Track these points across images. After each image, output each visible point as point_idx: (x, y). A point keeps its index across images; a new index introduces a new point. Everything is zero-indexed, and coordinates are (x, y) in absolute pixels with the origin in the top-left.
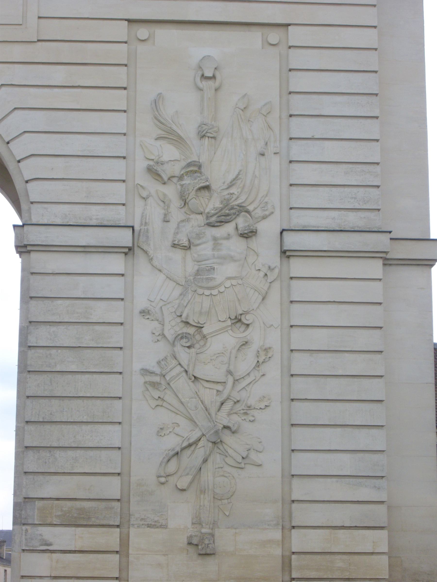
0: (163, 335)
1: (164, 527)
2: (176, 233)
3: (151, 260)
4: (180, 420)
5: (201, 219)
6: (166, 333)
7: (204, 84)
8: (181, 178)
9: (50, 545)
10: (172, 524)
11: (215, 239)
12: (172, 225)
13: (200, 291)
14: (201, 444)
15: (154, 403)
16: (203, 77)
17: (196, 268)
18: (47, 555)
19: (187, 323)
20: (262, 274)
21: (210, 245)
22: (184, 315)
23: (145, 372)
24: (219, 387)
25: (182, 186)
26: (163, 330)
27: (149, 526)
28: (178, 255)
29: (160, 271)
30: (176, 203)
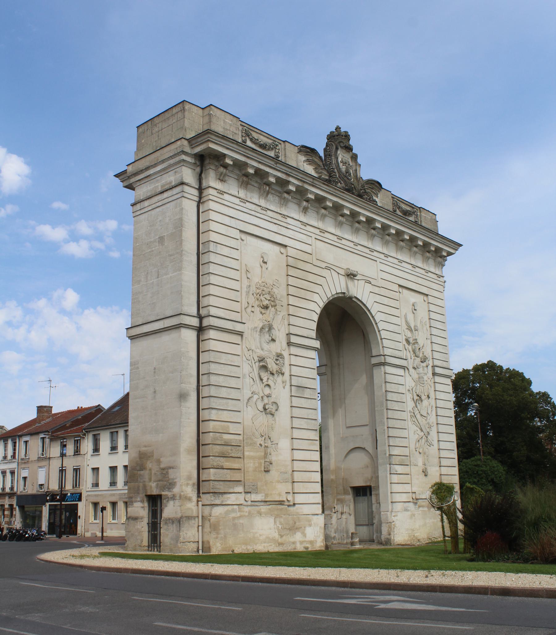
0: (413, 399)
1: (417, 466)
2: (413, 363)
3: (409, 373)
4: (419, 430)
5: (418, 360)
6: (414, 398)
7: (414, 311)
8: (414, 344)
9: (397, 472)
11: (423, 367)
12: (412, 360)
13: (421, 385)
14: (423, 437)
15: (413, 422)
17: (418, 376)
18: (397, 475)
20: (430, 380)
21: (421, 369)
22: (417, 393)
23: (410, 412)
24: (425, 418)
25: (415, 347)
26: (413, 397)
27: (415, 465)
28: (413, 370)
29: (411, 376)
30: (412, 353)
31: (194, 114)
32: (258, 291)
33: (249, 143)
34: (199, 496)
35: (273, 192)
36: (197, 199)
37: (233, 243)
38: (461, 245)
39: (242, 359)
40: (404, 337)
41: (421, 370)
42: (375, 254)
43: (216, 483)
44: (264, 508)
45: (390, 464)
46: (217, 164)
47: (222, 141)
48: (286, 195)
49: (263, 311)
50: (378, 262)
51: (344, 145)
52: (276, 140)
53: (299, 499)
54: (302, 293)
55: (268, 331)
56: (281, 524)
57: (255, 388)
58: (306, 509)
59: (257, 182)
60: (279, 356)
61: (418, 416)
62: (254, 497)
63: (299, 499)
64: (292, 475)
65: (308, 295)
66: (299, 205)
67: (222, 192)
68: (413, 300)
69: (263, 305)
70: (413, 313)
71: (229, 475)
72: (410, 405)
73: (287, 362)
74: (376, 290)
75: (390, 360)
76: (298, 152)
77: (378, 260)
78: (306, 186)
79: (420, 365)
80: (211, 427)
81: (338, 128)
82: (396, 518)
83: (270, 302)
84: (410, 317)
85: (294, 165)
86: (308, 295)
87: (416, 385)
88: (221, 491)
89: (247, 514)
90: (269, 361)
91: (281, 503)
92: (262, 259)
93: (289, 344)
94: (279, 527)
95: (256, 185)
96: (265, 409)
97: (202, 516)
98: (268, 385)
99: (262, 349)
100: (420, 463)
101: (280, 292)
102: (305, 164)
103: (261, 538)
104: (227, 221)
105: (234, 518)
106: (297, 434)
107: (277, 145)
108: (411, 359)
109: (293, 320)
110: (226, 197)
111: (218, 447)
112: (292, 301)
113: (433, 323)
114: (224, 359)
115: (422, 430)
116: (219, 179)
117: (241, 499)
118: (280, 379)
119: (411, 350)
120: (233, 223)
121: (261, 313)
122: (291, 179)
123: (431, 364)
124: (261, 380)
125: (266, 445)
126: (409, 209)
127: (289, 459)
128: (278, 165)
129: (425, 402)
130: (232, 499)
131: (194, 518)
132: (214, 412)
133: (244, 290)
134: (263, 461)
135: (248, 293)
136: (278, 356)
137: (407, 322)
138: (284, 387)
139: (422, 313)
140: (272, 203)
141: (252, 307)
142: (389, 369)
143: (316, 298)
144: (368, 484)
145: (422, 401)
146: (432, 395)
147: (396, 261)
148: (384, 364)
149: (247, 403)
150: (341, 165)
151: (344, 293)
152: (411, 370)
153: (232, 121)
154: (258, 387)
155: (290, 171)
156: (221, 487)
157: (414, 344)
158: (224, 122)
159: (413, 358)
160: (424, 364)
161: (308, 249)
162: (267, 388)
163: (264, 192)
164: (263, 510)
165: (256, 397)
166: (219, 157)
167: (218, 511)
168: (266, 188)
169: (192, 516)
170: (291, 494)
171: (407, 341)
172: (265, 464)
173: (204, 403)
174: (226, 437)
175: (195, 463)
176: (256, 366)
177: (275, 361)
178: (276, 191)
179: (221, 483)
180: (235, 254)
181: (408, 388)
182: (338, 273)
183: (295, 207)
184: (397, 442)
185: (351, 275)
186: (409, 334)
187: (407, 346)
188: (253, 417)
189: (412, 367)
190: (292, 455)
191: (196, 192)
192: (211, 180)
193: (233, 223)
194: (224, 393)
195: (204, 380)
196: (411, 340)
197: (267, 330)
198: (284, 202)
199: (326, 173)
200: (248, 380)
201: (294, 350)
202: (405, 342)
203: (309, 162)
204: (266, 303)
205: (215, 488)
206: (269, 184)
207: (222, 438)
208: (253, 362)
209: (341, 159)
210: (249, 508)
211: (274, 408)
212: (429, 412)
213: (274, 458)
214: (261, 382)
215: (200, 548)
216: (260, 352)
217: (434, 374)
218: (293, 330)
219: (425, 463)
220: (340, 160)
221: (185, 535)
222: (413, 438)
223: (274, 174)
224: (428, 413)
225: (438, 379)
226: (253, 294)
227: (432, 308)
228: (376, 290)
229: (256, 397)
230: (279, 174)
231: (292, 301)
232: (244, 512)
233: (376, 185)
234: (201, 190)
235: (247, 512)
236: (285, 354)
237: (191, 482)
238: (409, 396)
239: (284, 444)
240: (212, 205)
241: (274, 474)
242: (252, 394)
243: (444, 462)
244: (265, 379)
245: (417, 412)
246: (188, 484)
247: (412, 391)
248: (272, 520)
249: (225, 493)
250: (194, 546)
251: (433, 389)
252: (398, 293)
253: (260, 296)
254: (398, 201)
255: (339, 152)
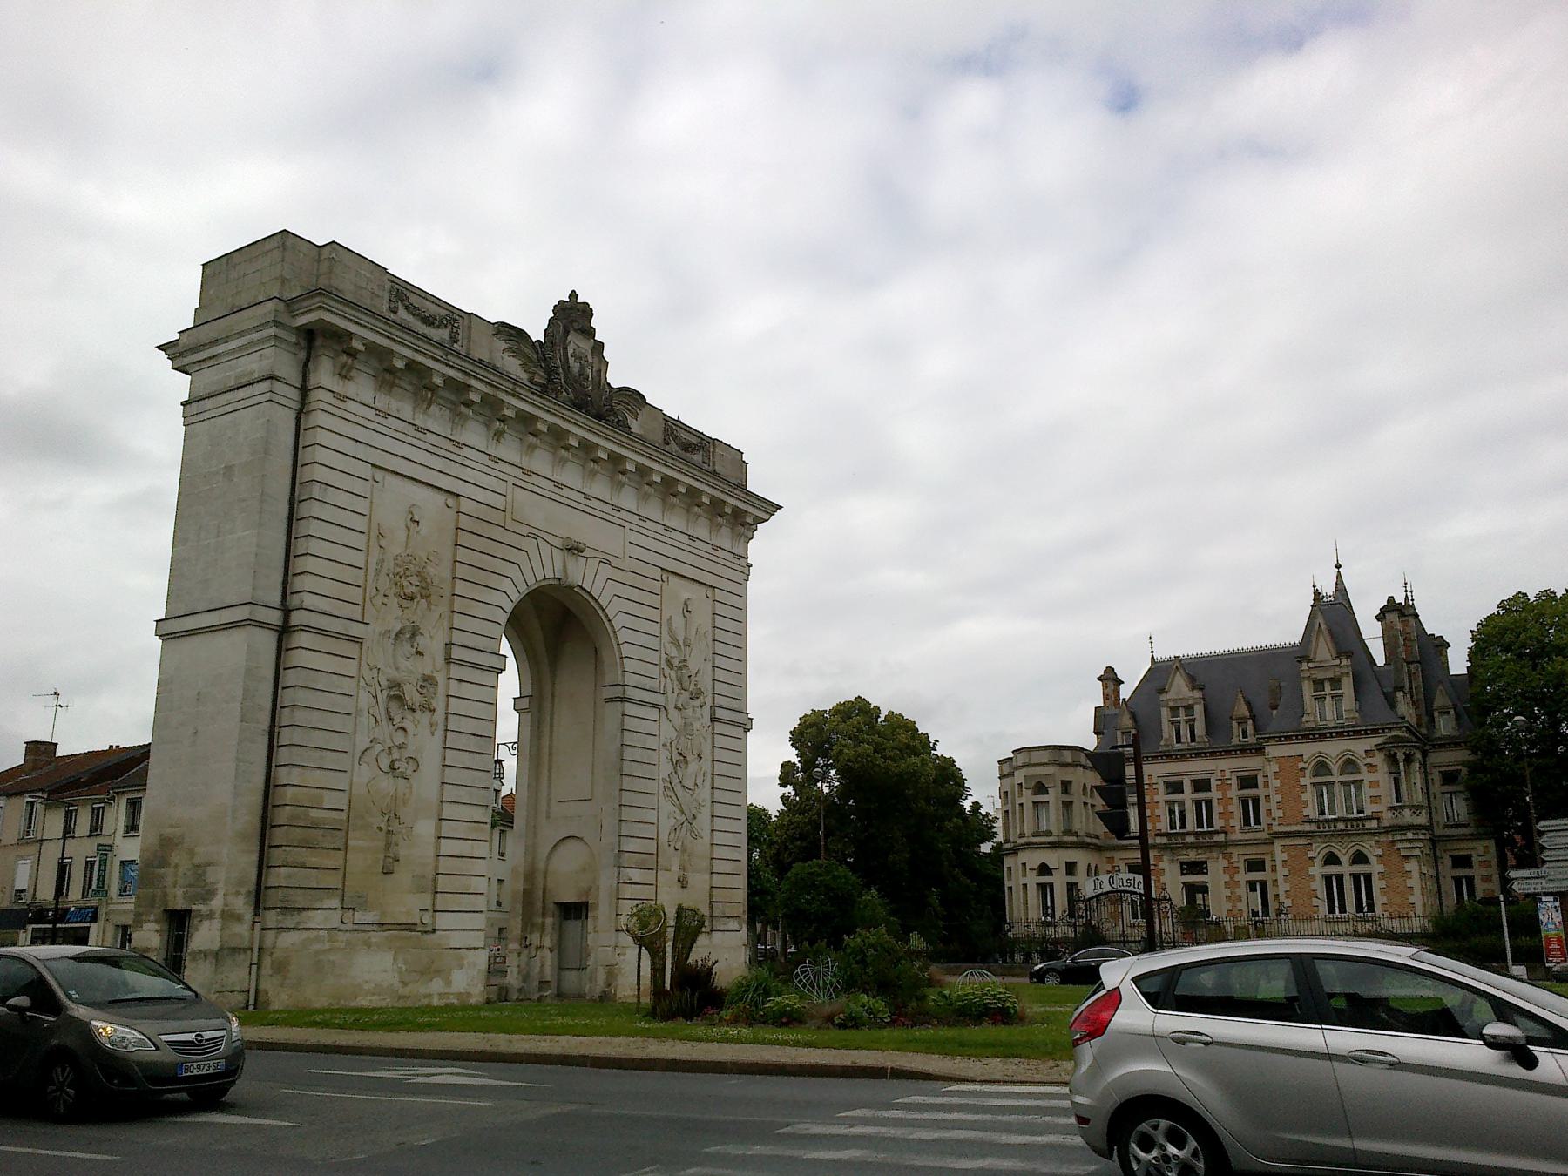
0: (671, 759)
1: (670, 870)
2: (677, 701)
4: (678, 811)
5: (687, 694)
7: (686, 614)
8: (680, 668)
10: (672, 870)
11: (693, 707)
16: (687, 611)
19: (681, 754)
21: (691, 710)
23: (664, 780)
30: (676, 683)
31: (302, 255)
32: (398, 570)
33: (403, 314)
34: (256, 914)
35: (442, 402)
36: (296, 406)
37: (358, 486)
38: (781, 507)
39: (358, 685)
40: (664, 656)
41: (689, 712)
42: (623, 514)
43: (291, 891)
44: (377, 937)
45: (619, 867)
46: (336, 347)
47: (347, 310)
48: (463, 409)
49: (405, 603)
50: (627, 528)
51: (580, 326)
52: (455, 311)
53: (443, 921)
54: (481, 577)
55: (411, 638)
56: (405, 963)
57: (378, 733)
58: (456, 940)
59: (411, 384)
60: (428, 680)
61: (678, 788)
62: (359, 917)
63: (443, 921)
64: (435, 880)
65: (493, 581)
66: (488, 426)
67: (344, 398)
68: (686, 595)
69: (405, 595)
70: (684, 616)
71: (314, 879)
72: (666, 768)
73: (441, 690)
74: (619, 576)
75: (631, 693)
76: (494, 335)
77: (628, 526)
78: (501, 395)
79: (688, 704)
80: (289, 796)
81: (573, 295)
82: (622, 958)
83: (418, 588)
84: (678, 622)
85: (485, 358)
86: (493, 581)
87: (678, 737)
88: (297, 906)
89: (343, 945)
90: (406, 687)
91: (410, 927)
92: (410, 516)
93: (449, 660)
94: (401, 968)
95: (408, 387)
96: (392, 768)
97: (260, 949)
98: (404, 729)
99: (397, 669)
100: (675, 868)
101: (439, 573)
102: (505, 355)
103: (366, 987)
104: (349, 447)
105: (317, 953)
106: (448, 811)
107: (455, 320)
108: (673, 692)
109: (459, 621)
110: (351, 405)
111: (298, 830)
112: (460, 588)
113: (720, 635)
114: (322, 682)
115: (683, 812)
116: (340, 375)
117: (333, 919)
118: (425, 718)
119: (674, 678)
120: (361, 451)
121: (401, 607)
122: (473, 382)
123: (709, 702)
124: (391, 719)
125: (389, 828)
126: (694, 440)
127: (431, 853)
128: (450, 357)
129: (693, 765)
130: (316, 919)
131: (245, 950)
132: (296, 771)
133: (372, 567)
134: (382, 856)
135: (378, 572)
136: (424, 681)
137: (671, 631)
138: (433, 733)
139: (702, 618)
140: (436, 420)
141: (385, 596)
142: (630, 709)
143: (506, 585)
144: (584, 899)
145: (687, 763)
146: (706, 754)
147: (660, 529)
148: (622, 699)
149: (360, 758)
150: (571, 360)
151: (560, 579)
152: (673, 712)
153: (371, 273)
154: (385, 731)
155: (471, 367)
156: (300, 899)
157: (680, 668)
158: (358, 273)
159: (677, 691)
160: (697, 703)
161: (498, 501)
162: (401, 733)
163: (424, 401)
164: (373, 940)
165: (378, 747)
166: (339, 337)
167: (288, 940)
168: (427, 394)
169: (242, 946)
170: (431, 913)
171: (670, 663)
172: (384, 861)
173: (283, 756)
174: (314, 813)
175: (255, 857)
176: (382, 698)
177: (420, 690)
178: (446, 400)
179: (299, 891)
180: (361, 505)
181: (663, 740)
182: (551, 545)
183: (482, 429)
184: (636, 830)
185: (574, 549)
186: (674, 652)
187: (667, 671)
188: (370, 782)
189: (673, 706)
190: (438, 847)
191: (294, 394)
192: (324, 374)
193: (361, 451)
194: (317, 739)
195: (285, 717)
196: (676, 662)
197: (408, 636)
198: (457, 418)
199: (543, 374)
200: (365, 720)
201: (456, 671)
202: (664, 665)
203: (514, 352)
204: (410, 590)
205: (287, 901)
206: (433, 389)
207: (308, 815)
208: (378, 689)
209: (572, 351)
210: (348, 934)
211: (412, 765)
212: (699, 782)
213: (402, 852)
214: (390, 723)
215: (252, 1001)
216: (393, 674)
217: (713, 719)
218: (458, 637)
219: (684, 867)
220: (570, 351)
221: (225, 979)
222: (666, 825)
223: (442, 372)
224: (696, 784)
225: (719, 728)
226: (388, 575)
227: (720, 609)
228: (619, 576)
229: (378, 747)
230: (451, 373)
231: (460, 588)
232: (338, 941)
233: (634, 398)
234: (304, 391)
235: (342, 942)
236: (440, 678)
237: (243, 890)
238: (665, 754)
239: (425, 828)
240: (320, 418)
241: (403, 876)
242: (371, 742)
243: (720, 866)
244: (397, 719)
245: (676, 781)
246: (238, 893)
247: (671, 746)
248: (389, 957)
249: (305, 909)
250: (241, 998)
251: (709, 741)
252: (661, 582)
253: (401, 577)
254: (674, 427)
255: (569, 338)
